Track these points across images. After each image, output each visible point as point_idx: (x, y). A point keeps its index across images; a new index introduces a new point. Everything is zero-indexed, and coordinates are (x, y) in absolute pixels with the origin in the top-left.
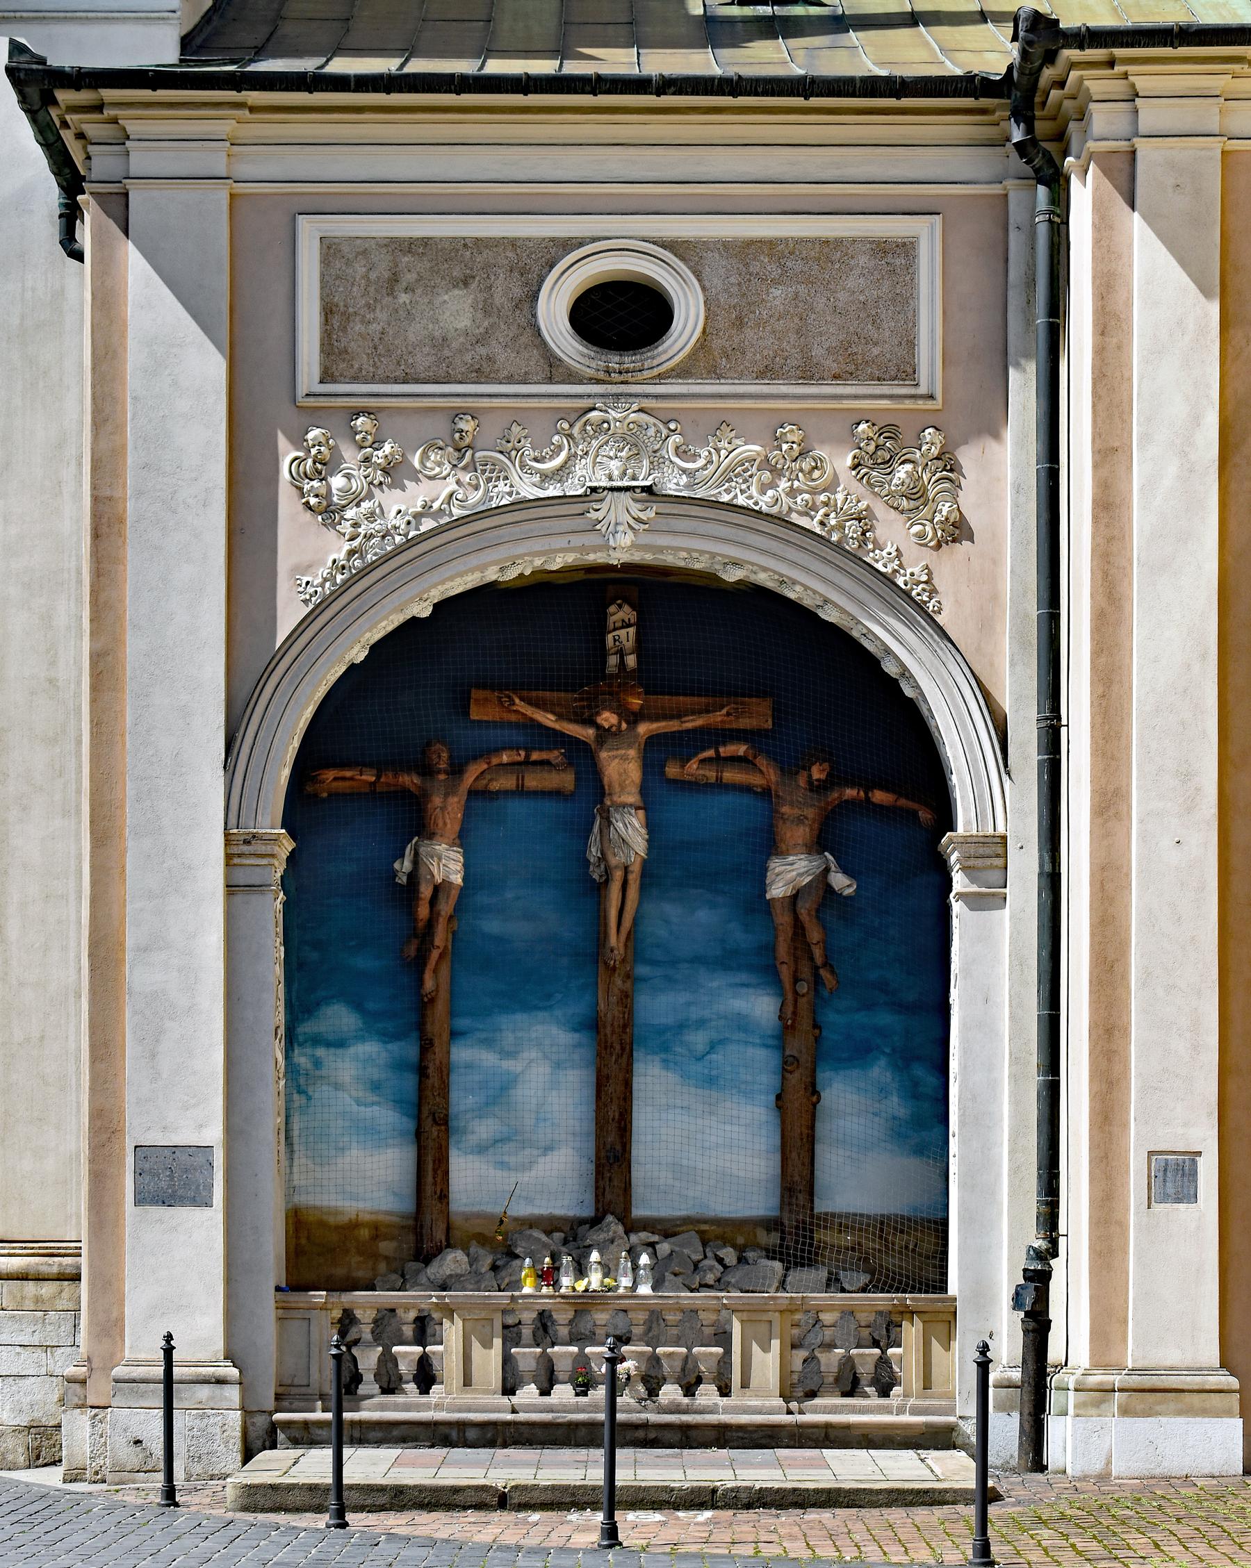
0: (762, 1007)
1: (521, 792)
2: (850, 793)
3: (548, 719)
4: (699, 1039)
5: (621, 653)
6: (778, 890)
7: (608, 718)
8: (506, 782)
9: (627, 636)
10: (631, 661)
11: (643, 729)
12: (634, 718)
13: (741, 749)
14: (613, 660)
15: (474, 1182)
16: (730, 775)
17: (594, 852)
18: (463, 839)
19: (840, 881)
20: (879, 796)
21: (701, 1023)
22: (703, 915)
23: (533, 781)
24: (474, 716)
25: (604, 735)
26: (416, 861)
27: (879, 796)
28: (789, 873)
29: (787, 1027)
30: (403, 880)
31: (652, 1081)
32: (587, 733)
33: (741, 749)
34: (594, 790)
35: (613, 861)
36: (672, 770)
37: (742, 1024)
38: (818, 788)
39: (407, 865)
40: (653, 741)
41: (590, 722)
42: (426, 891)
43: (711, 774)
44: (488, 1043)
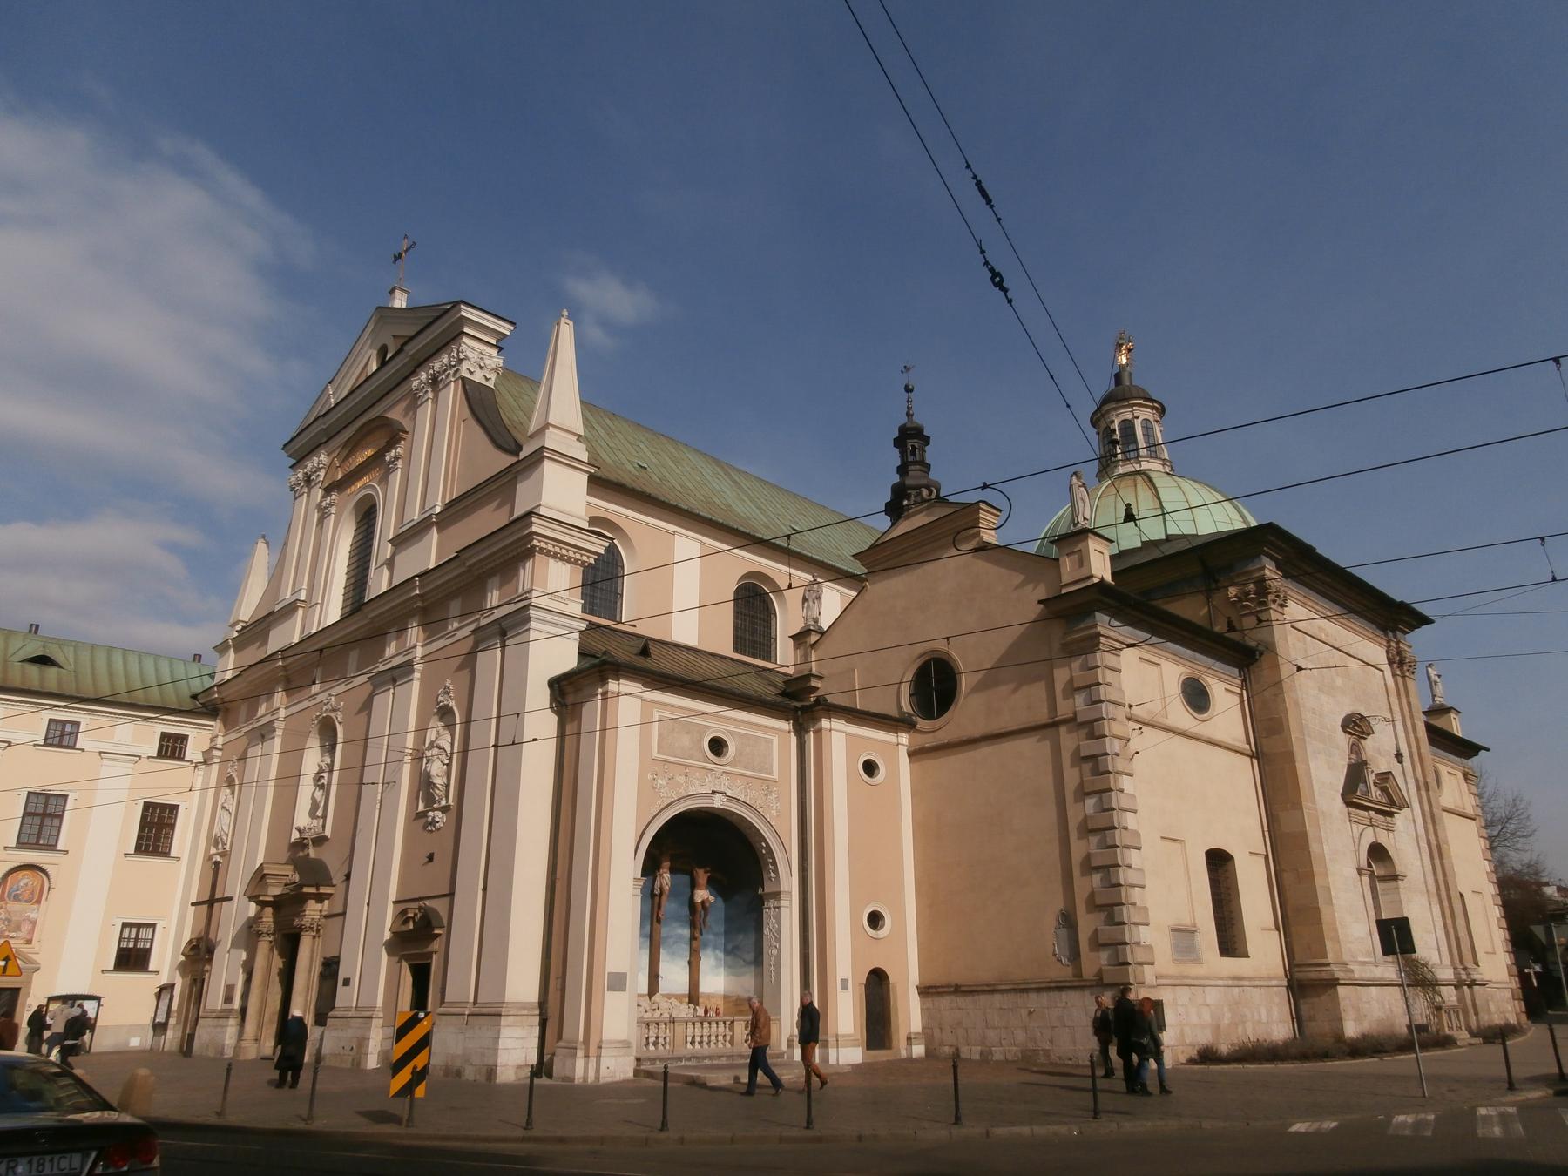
28: (702, 895)
37: (681, 937)
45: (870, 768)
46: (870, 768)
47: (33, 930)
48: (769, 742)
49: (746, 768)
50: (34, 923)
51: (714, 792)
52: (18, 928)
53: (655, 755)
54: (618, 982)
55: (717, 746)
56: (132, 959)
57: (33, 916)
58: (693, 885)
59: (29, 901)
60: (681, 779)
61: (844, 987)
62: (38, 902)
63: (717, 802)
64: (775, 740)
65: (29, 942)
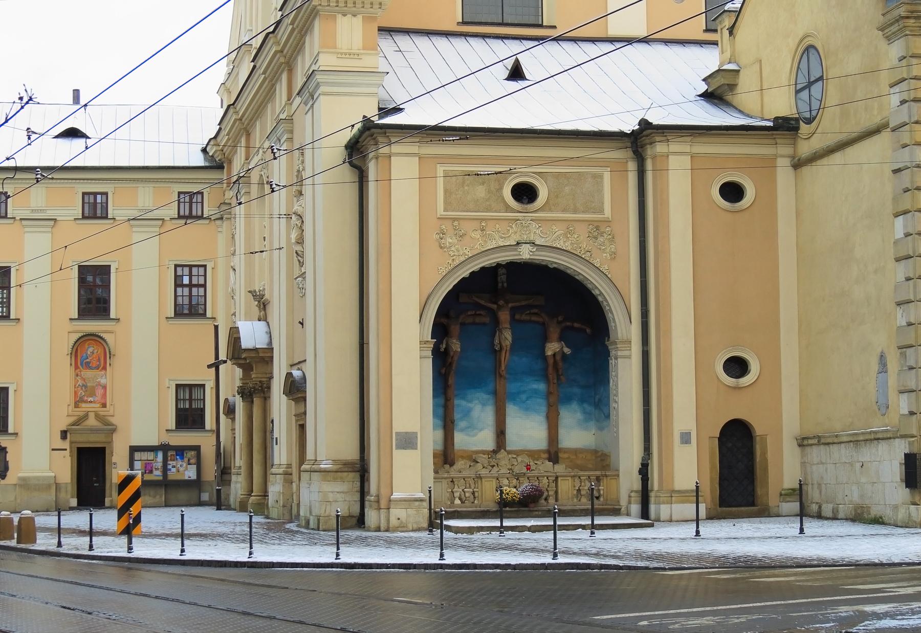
0: (541, 386)
1: (474, 324)
2: (568, 324)
3: (483, 302)
4: (524, 397)
5: (503, 283)
6: (549, 353)
7: (501, 302)
8: (470, 320)
9: (504, 278)
10: (505, 285)
11: (510, 305)
12: (507, 302)
13: (536, 311)
14: (500, 285)
15: (461, 440)
16: (534, 318)
17: (497, 341)
18: (460, 339)
19: (567, 350)
20: (576, 325)
21: (524, 392)
22: (524, 359)
23: (478, 320)
24: (461, 300)
25: (499, 307)
26: (447, 344)
27: (576, 325)
28: (552, 348)
29: (549, 394)
30: (442, 350)
31: (512, 410)
32: (494, 306)
33: (536, 311)
34: (496, 322)
35: (504, 345)
36: (517, 317)
37: (536, 392)
38: (559, 323)
39: (444, 346)
40: (512, 309)
41: (495, 303)
42: (452, 354)
43: (527, 318)
44: (463, 398)
45: (732, 192)
46: (732, 192)
47: (104, 395)
48: (598, 178)
49: (564, 211)
50: (105, 388)
51: (518, 244)
52: (93, 394)
53: (441, 211)
54: (408, 441)
55: (525, 193)
56: (189, 417)
57: (103, 381)
58: (545, 339)
59: (97, 368)
60: (477, 235)
61: (686, 438)
62: (105, 368)
63: (525, 254)
64: (607, 176)
65: (104, 405)
